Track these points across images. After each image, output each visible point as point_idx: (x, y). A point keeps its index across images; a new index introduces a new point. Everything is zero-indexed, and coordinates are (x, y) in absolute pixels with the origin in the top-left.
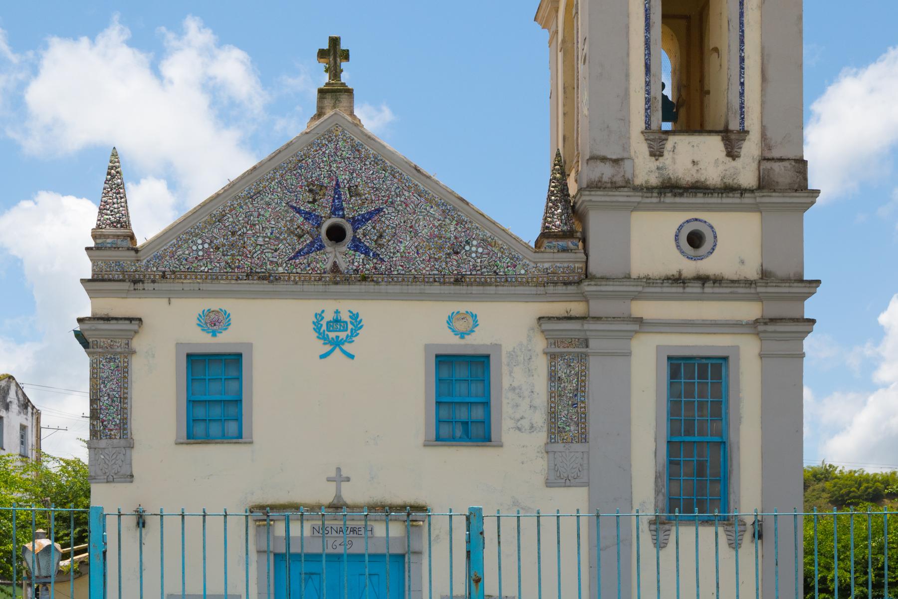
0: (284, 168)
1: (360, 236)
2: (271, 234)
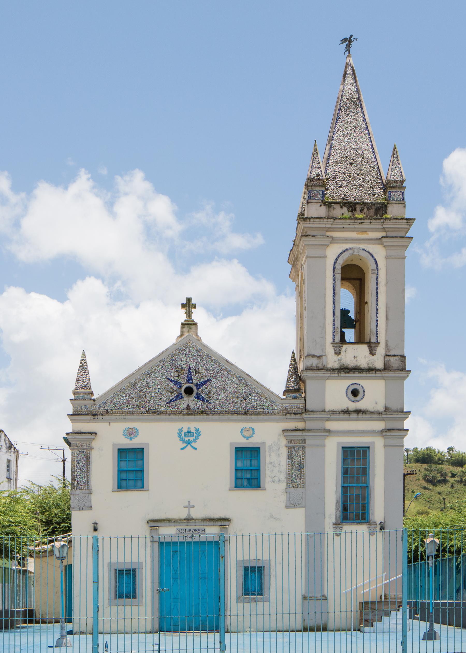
2: (158, 391)
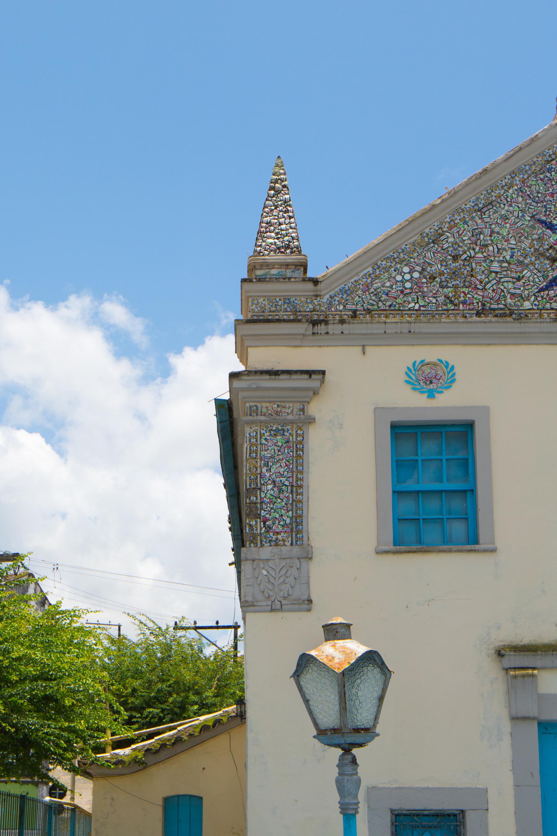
0: (526, 172)
2: (512, 257)
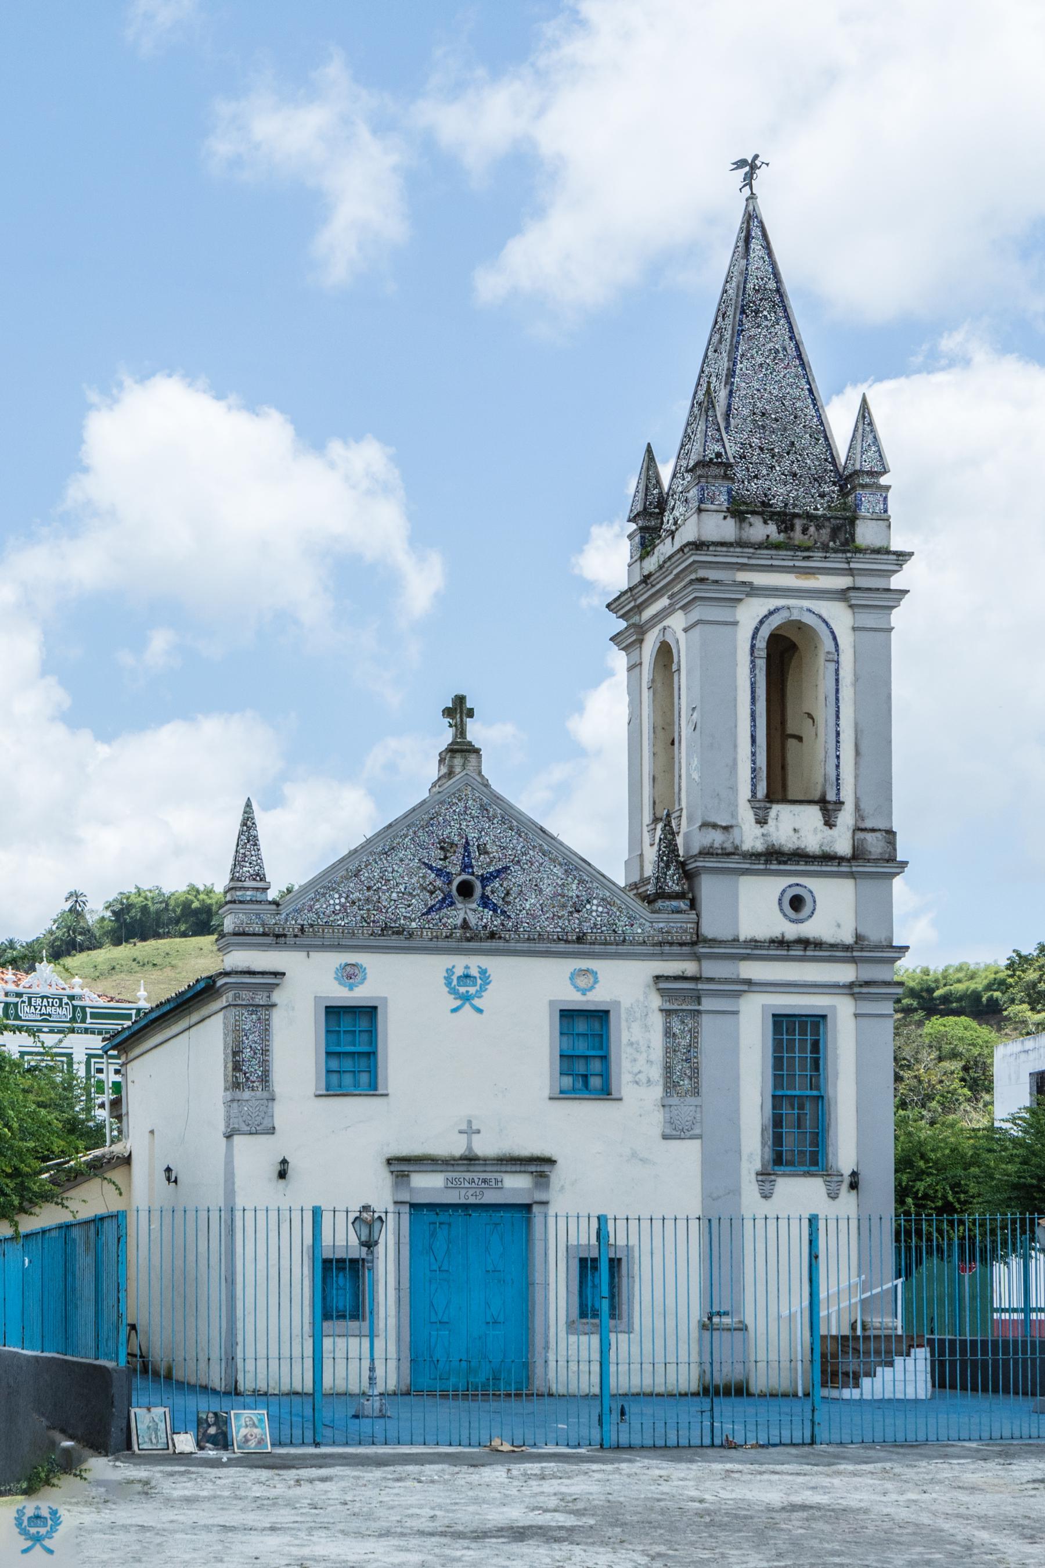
1: (488, 893)
